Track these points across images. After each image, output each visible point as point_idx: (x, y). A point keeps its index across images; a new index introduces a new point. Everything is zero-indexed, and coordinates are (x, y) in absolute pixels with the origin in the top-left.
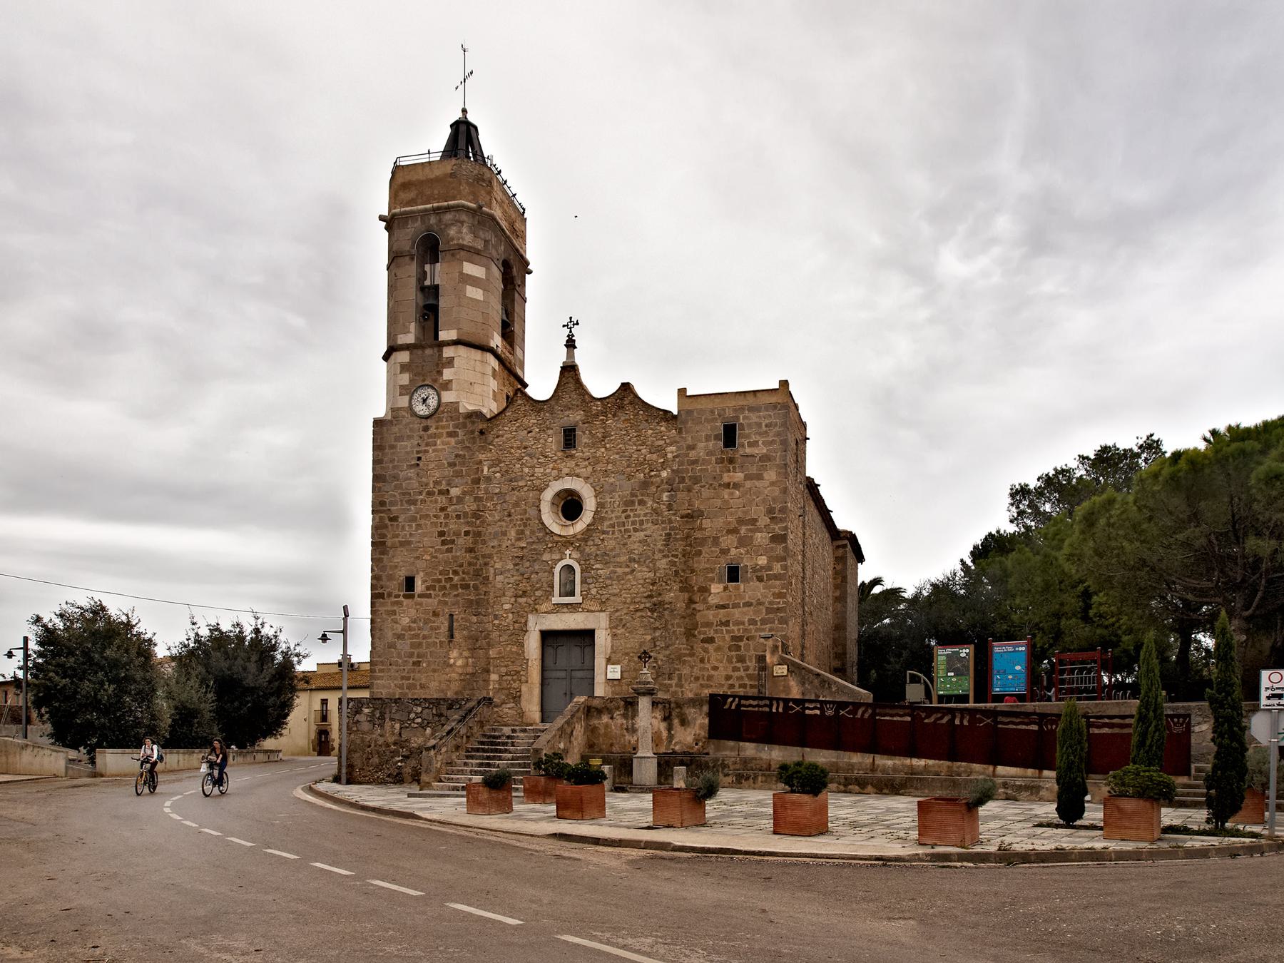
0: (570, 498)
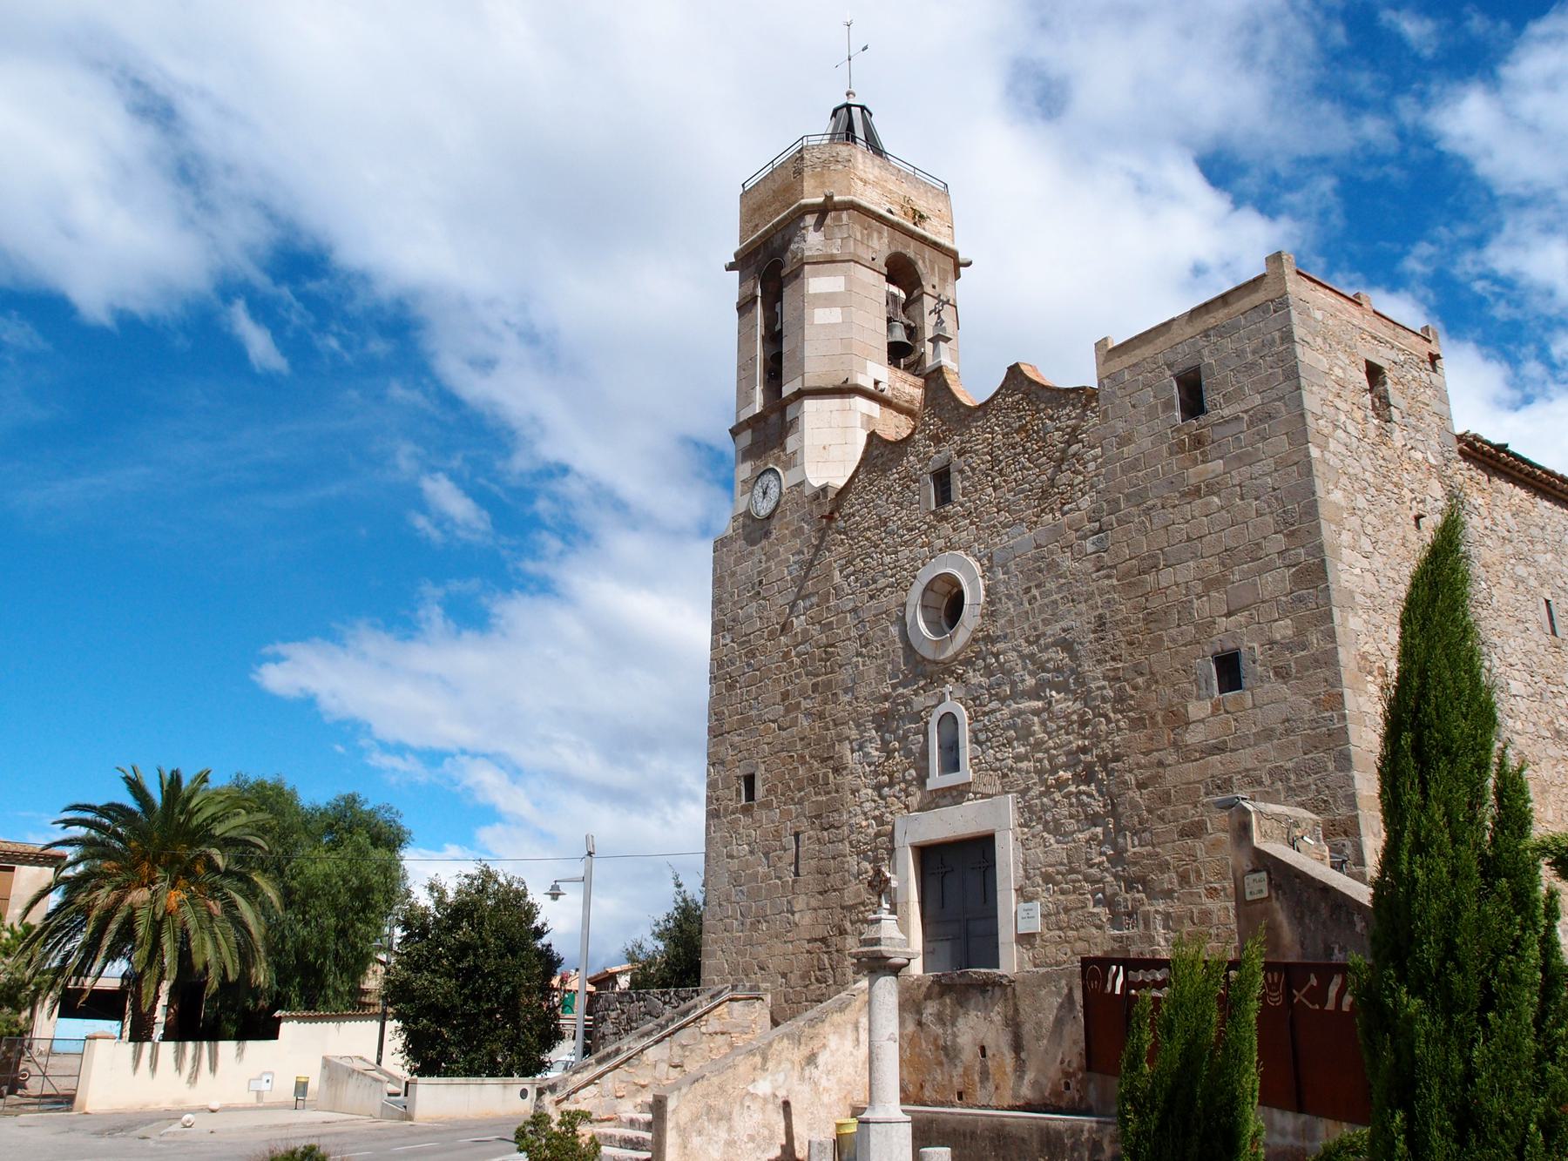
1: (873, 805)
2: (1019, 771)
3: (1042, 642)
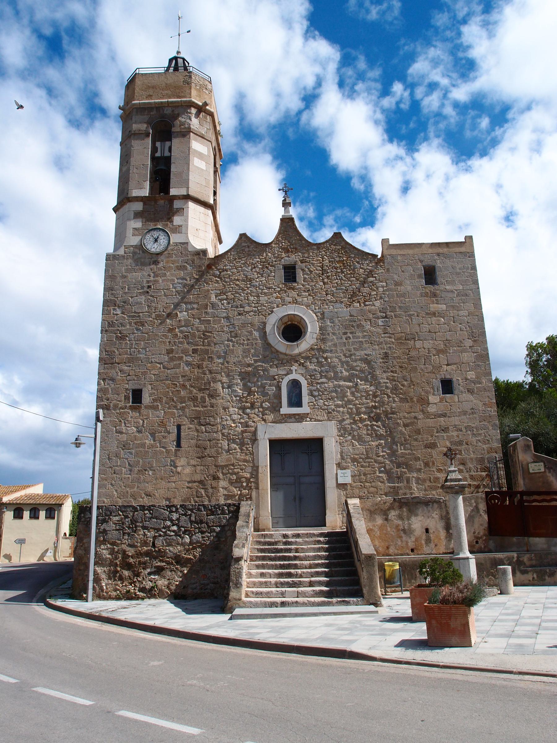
0: (289, 323)
1: (239, 416)
2: (338, 412)
3: (353, 357)
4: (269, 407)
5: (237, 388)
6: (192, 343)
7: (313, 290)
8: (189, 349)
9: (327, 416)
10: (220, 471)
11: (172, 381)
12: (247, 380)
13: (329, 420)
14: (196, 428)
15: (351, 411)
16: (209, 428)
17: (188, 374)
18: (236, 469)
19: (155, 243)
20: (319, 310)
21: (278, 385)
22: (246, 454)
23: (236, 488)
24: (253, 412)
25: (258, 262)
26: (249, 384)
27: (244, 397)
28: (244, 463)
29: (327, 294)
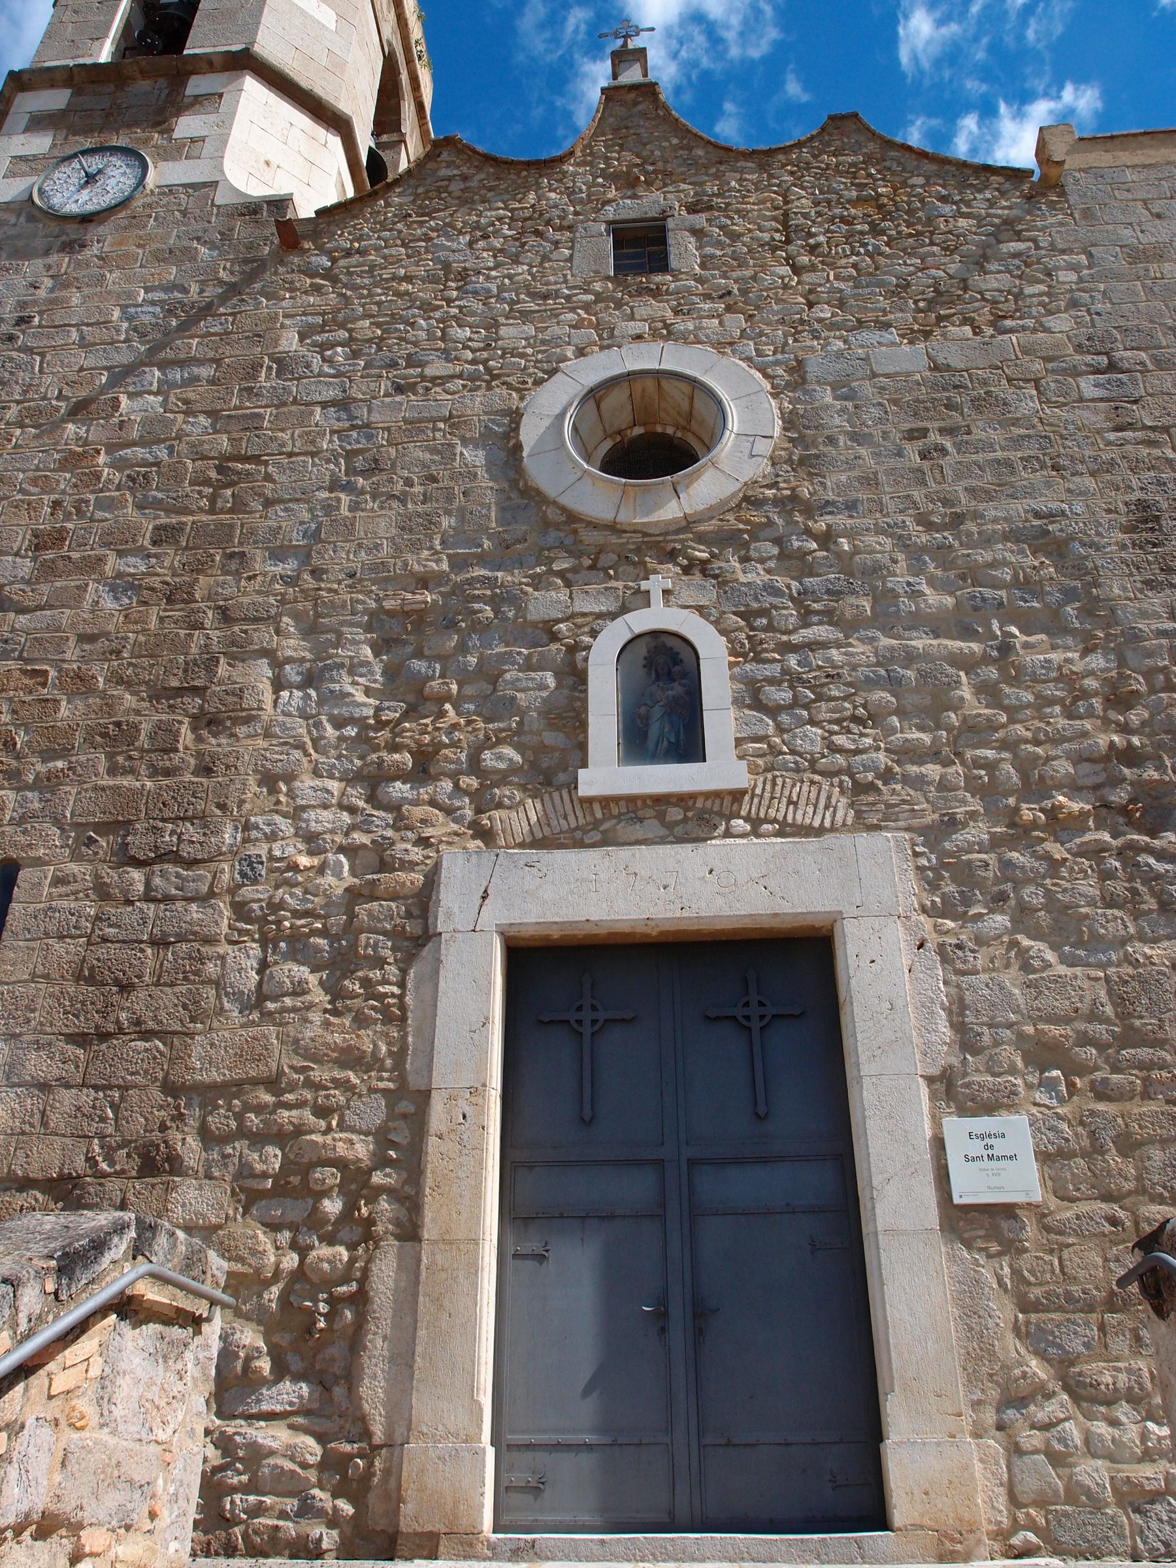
0: (638, 431)
1: (346, 817)
2: (919, 782)
3: (971, 526)
4: (514, 769)
5: (354, 683)
6: (157, 504)
7: (744, 292)
8: (138, 528)
9: (852, 805)
10: (193, 1123)
11: (27, 661)
12: (410, 649)
13: (862, 824)
14: (97, 876)
15: (992, 776)
16: (166, 878)
17: (111, 628)
18: (288, 1106)
19: (83, 187)
20: (779, 356)
21: (573, 665)
22: (361, 1021)
23: (273, 1227)
24: (425, 792)
25: (500, 219)
26: (418, 665)
27: (381, 725)
28: (338, 1074)
29: (811, 305)
